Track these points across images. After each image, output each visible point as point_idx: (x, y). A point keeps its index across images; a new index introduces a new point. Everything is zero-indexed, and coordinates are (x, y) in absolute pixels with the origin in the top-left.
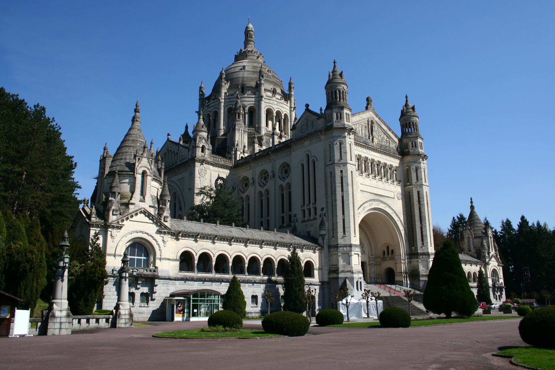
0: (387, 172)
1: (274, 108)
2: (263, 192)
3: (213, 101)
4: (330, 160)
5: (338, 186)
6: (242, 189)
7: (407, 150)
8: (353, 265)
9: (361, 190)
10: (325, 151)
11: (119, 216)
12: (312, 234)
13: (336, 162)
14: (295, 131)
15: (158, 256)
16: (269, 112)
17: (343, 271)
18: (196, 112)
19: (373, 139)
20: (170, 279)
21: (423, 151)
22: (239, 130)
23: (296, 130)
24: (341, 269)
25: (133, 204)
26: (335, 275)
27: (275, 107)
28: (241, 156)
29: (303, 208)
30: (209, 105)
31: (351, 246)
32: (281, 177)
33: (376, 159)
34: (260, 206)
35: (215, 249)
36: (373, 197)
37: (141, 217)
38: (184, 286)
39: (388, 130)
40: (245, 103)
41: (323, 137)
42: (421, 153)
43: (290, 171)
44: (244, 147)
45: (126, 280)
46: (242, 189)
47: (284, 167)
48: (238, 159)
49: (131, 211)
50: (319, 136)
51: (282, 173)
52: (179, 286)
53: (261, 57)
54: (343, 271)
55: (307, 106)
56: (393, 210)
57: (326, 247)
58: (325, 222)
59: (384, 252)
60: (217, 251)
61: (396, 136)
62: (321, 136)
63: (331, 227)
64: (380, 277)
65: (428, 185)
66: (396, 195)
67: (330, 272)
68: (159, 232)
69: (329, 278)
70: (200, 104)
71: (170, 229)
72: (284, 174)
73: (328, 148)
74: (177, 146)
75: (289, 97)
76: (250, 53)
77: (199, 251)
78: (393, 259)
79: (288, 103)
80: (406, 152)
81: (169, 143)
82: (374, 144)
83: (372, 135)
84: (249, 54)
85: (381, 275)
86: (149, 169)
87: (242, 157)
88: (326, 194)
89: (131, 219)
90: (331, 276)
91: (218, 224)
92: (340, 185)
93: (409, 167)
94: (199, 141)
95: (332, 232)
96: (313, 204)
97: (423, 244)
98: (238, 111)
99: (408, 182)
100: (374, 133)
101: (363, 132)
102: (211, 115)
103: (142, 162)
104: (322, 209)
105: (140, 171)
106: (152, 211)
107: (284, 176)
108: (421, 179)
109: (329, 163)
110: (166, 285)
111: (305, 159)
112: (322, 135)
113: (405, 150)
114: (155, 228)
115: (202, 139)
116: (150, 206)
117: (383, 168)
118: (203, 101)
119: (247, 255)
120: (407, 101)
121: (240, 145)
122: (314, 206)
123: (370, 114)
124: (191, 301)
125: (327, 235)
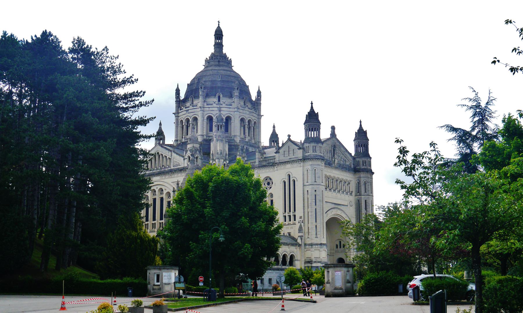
0: (344, 185)
1: (246, 117)
3: (193, 108)
4: (307, 182)
5: (313, 201)
9: (326, 202)
10: (303, 174)
12: (292, 234)
16: (242, 120)
17: (315, 262)
18: (173, 113)
19: (335, 160)
26: (309, 265)
27: (247, 116)
28: (224, 163)
29: (284, 215)
30: (188, 110)
31: (321, 244)
33: (336, 176)
36: (333, 206)
41: (302, 163)
43: (272, 183)
44: (226, 155)
47: (266, 180)
50: (300, 163)
51: (264, 184)
55: (289, 136)
56: (346, 215)
57: (303, 245)
58: (303, 227)
59: (337, 245)
63: (306, 230)
66: (349, 204)
67: (306, 262)
69: (305, 267)
70: (176, 107)
72: (267, 185)
73: (306, 173)
74: (170, 153)
75: (257, 105)
79: (256, 112)
80: (358, 168)
83: (334, 157)
87: (225, 164)
88: (304, 207)
90: (306, 265)
92: (314, 201)
93: (360, 181)
95: (307, 234)
96: (293, 213)
98: (221, 124)
99: (358, 192)
100: (336, 155)
102: (191, 120)
104: (301, 217)
107: (267, 187)
108: (369, 191)
109: (306, 184)
111: (287, 178)
113: (357, 166)
115: (197, 151)
117: (340, 183)
118: (179, 104)
120: (361, 125)
121: (223, 153)
122: (294, 214)
123: (333, 140)
125: (304, 236)
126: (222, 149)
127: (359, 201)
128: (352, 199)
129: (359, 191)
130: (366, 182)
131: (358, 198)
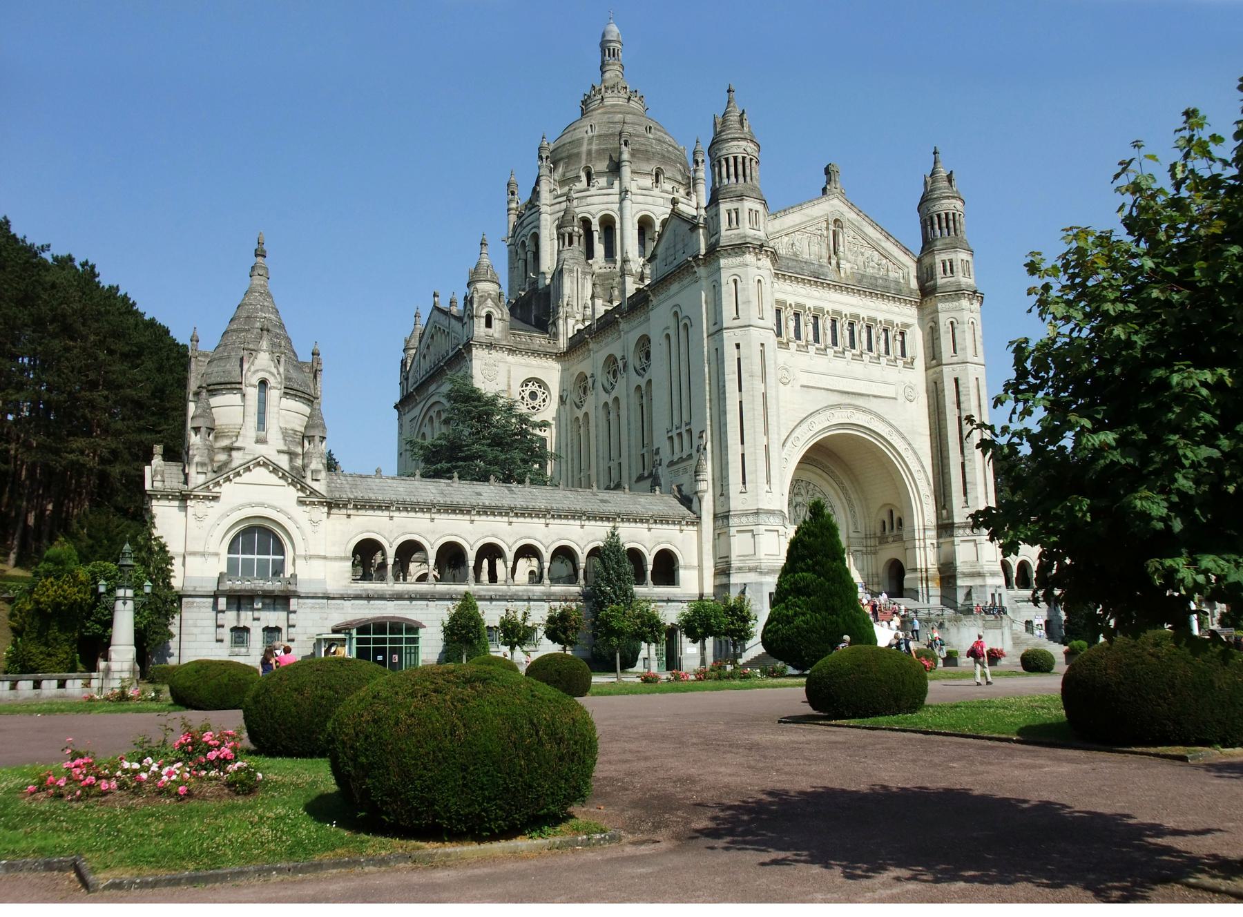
2: (610, 402)
6: (577, 401)
7: (932, 283)
8: (762, 556)
11: (211, 475)
13: (725, 326)
14: (654, 263)
15: (300, 550)
17: (740, 569)
19: (838, 264)
20: (328, 598)
21: (971, 281)
22: (571, 271)
23: (657, 261)
24: (735, 563)
25: (239, 449)
26: (724, 580)
29: (670, 434)
32: (638, 368)
34: (606, 434)
35: (433, 532)
37: (261, 474)
38: (361, 611)
39: (884, 238)
40: (592, 209)
42: (963, 287)
45: (125, 604)
46: (577, 401)
48: (570, 335)
49: (235, 464)
52: (350, 610)
53: (636, 99)
54: (740, 569)
56: (891, 425)
60: (437, 536)
61: (906, 251)
62: (696, 269)
64: (876, 580)
65: (983, 362)
66: (901, 391)
68: (301, 502)
71: (324, 497)
76: (609, 91)
77: (396, 538)
78: (899, 538)
81: (436, 312)
82: (842, 275)
84: (607, 95)
85: (877, 575)
86: (273, 375)
89: (238, 479)
91: (456, 479)
94: (480, 304)
97: (966, 502)
98: (569, 229)
99: (934, 358)
101: (815, 249)
103: (257, 362)
105: (255, 380)
106: (283, 461)
108: (964, 349)
110: (318, 610)
111: (671, 322)
112: (698, 266)
113: (927, 282)
114: (293, 493)
116: (279, 452)
119: (510, 542)
124: (354, 641)
126: (572, 290)
127: (936, 383)
128: (917, 377)
129: (937, 356)
130: (956, 324)
131: (935, 373)
